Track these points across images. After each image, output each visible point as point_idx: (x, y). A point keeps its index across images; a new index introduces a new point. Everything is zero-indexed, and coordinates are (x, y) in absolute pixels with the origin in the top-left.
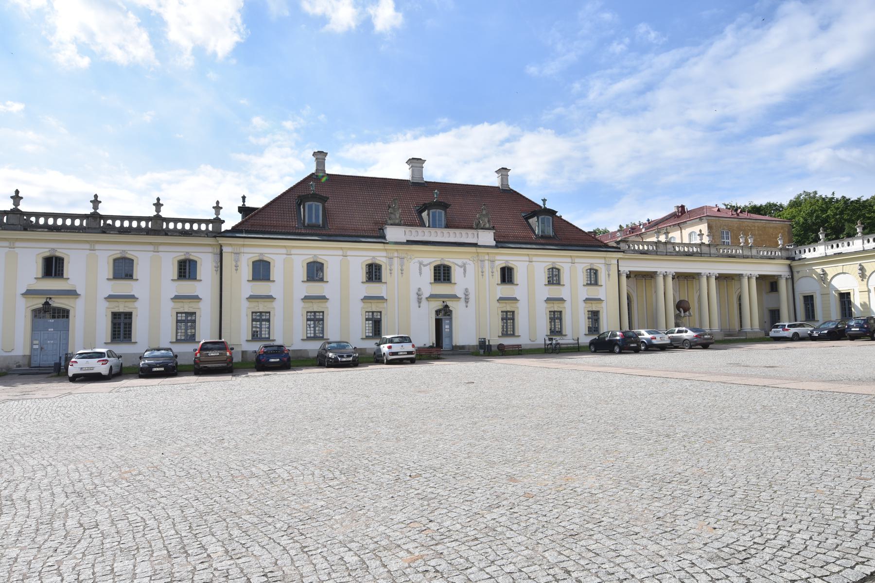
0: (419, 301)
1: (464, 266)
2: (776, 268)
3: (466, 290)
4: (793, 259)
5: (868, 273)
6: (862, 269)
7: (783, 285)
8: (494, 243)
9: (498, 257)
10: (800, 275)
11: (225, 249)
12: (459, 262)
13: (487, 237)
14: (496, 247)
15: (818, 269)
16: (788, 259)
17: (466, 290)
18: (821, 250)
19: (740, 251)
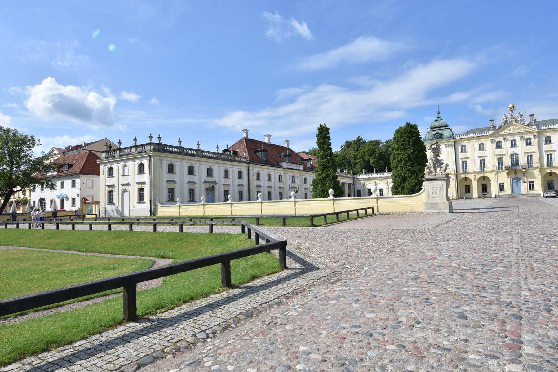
0: (290, 189)
1: (297, 177)
2: (350, 181)
3: (298, 185)
4: (354, 178)
5: (377, 184)
6: (375, 183)
7: (352, 186)
8: (303, 170)
9: (304, 175)
10: (357, 183)
11: (251, 168)
12: (297, 176)
13: (301, 168)
14: (304, 171)
15: (362, 182)
16: (353, 178)
17: (298, 185)
18: (363, 176)
19: (344, 175)
